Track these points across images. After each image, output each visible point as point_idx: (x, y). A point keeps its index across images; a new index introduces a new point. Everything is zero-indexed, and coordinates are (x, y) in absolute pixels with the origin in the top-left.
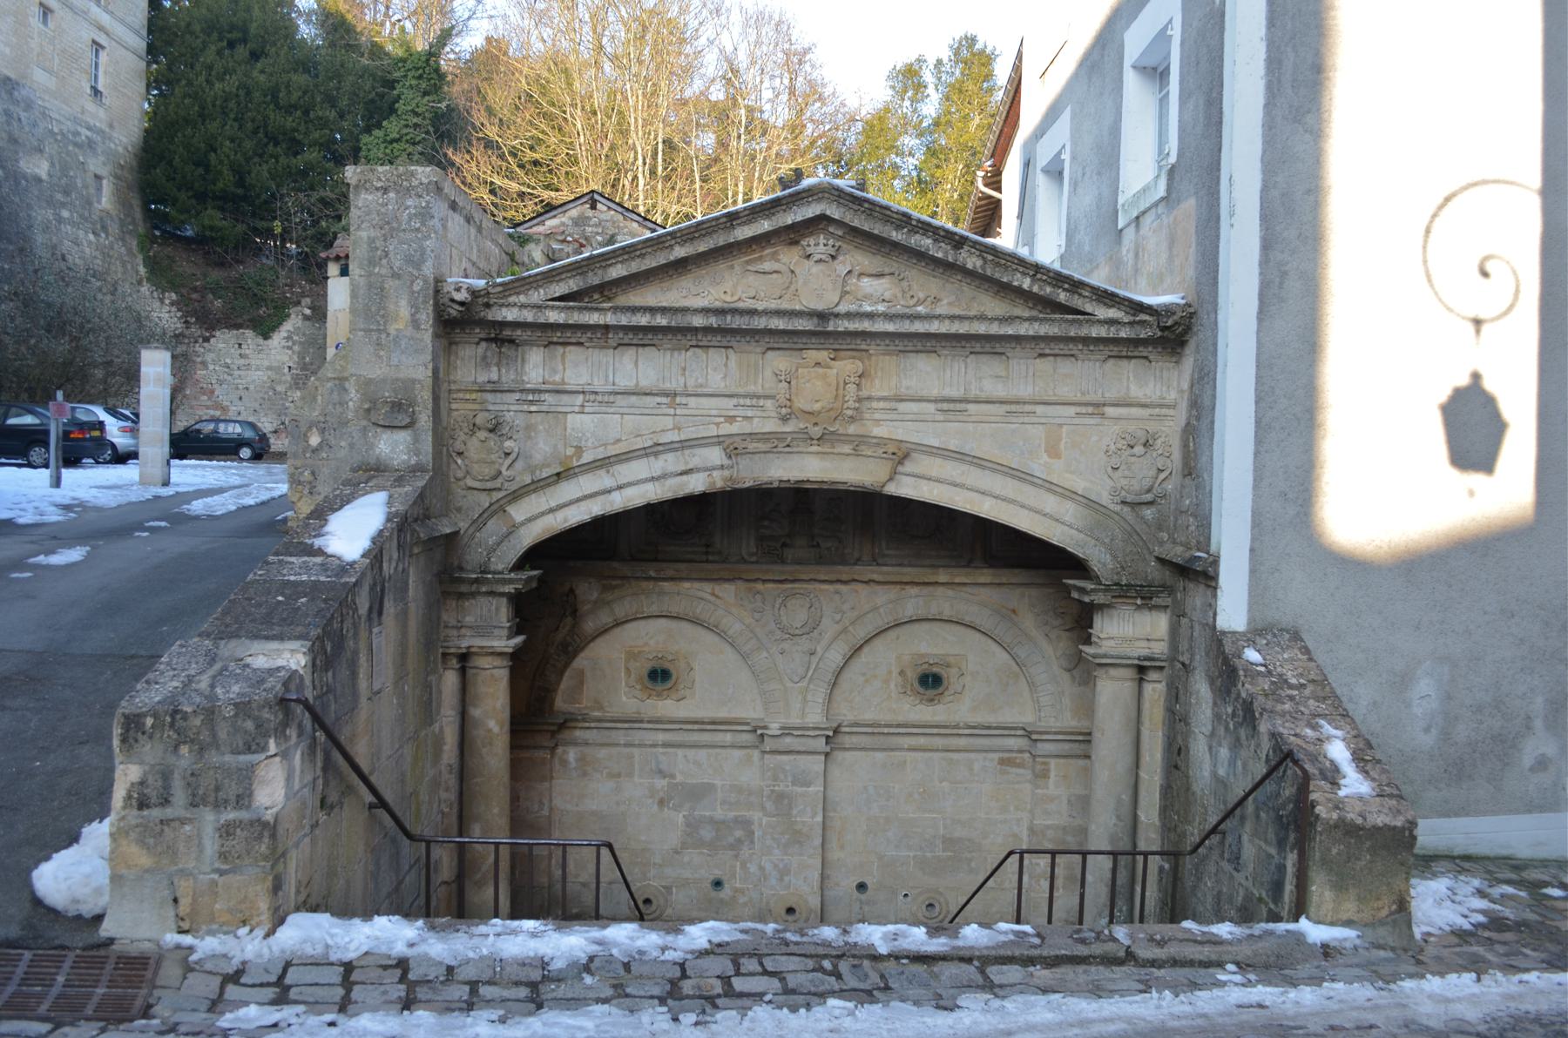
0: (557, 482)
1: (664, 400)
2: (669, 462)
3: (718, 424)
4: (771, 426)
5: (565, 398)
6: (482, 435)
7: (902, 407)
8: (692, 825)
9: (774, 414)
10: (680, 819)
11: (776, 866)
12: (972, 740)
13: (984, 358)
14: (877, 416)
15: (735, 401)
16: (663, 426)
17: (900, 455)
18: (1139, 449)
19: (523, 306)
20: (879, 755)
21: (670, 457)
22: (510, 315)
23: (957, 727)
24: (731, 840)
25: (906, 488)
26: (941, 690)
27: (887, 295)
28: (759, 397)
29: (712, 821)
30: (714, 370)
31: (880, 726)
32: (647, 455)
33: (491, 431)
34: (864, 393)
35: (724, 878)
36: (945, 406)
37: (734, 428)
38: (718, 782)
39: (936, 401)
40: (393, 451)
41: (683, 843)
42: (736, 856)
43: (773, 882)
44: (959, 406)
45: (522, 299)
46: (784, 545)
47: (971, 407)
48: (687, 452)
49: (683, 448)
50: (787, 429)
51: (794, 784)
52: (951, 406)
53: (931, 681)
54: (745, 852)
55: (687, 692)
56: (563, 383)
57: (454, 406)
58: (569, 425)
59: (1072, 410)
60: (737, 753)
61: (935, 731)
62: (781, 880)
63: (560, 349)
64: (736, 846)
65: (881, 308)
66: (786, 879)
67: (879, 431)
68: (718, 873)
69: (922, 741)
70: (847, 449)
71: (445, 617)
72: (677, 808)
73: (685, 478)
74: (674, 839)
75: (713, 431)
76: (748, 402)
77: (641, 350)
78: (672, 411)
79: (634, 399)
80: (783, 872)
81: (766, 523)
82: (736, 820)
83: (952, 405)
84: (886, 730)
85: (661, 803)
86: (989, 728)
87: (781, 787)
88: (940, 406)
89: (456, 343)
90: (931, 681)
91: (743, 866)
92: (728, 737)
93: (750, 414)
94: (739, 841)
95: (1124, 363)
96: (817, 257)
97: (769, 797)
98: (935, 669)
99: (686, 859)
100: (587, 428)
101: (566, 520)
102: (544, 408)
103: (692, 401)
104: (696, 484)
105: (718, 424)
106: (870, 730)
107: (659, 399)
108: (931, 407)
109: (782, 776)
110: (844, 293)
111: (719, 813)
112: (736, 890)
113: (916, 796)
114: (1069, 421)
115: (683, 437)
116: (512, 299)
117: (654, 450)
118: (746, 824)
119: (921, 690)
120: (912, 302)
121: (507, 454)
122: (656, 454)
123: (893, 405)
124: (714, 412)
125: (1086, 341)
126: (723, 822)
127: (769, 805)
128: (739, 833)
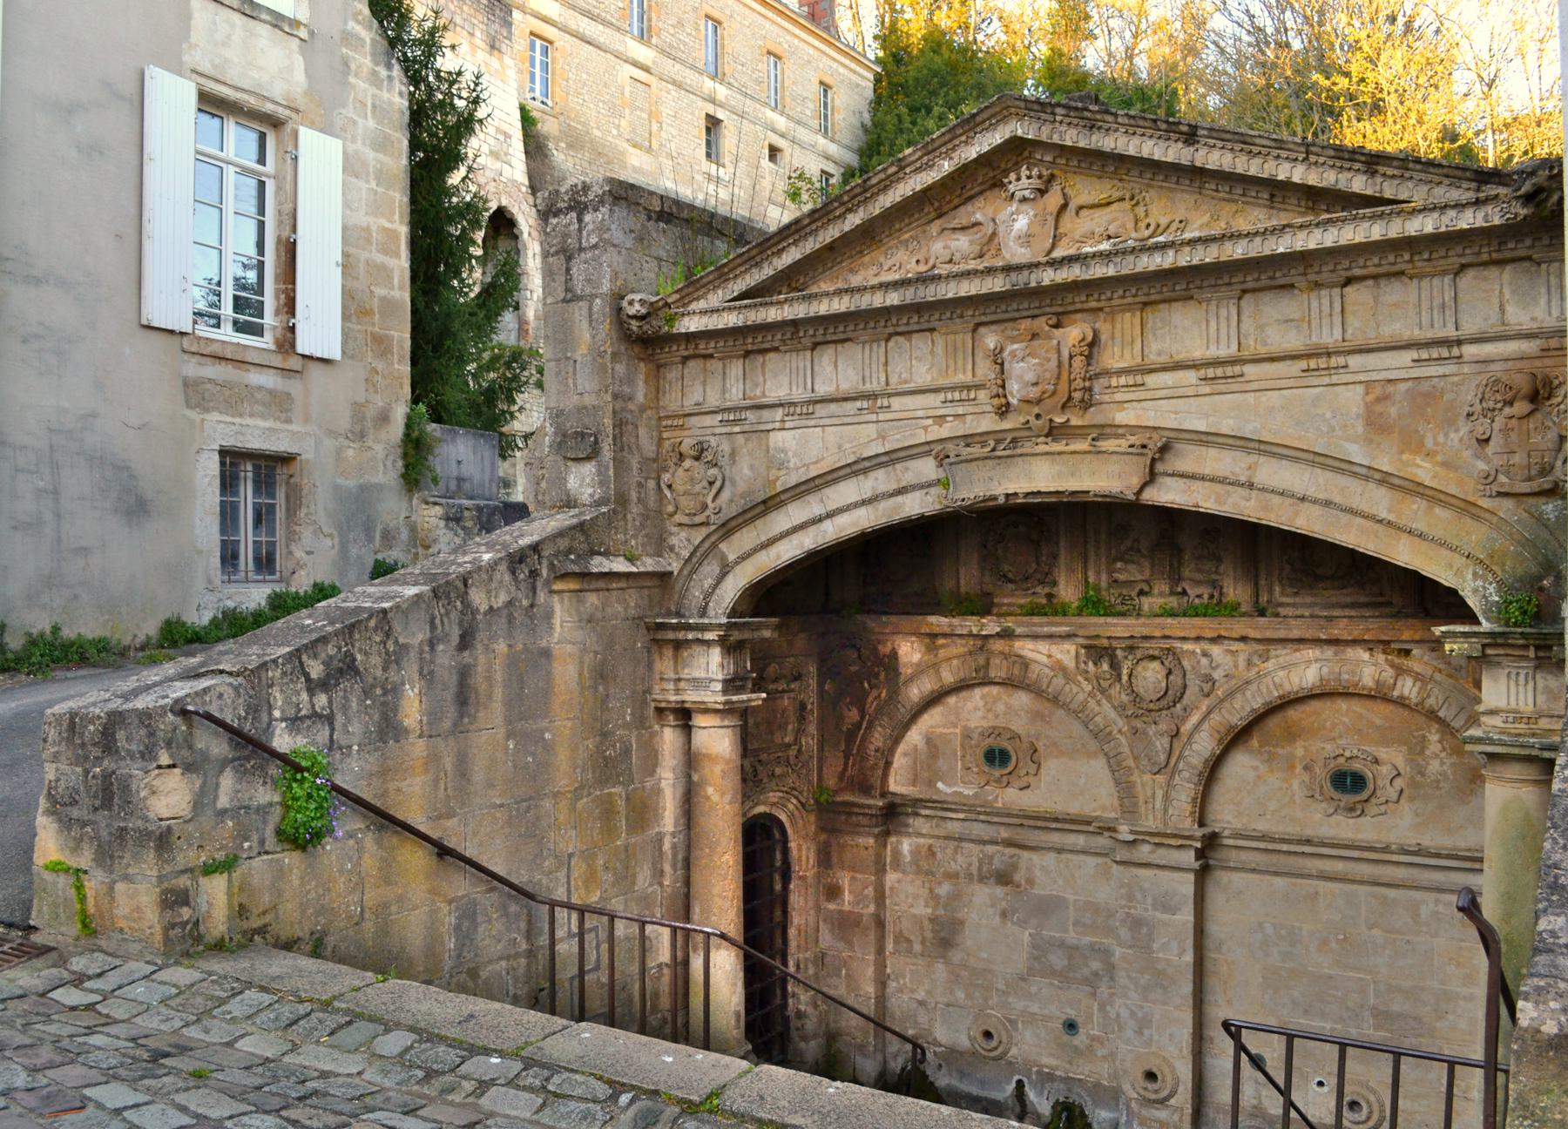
0: (763, 514)
1: (865, 404)
2: (879, 481)
3: (925, 428)
4: (988, 423)
5: (766, 414)
6: (687, 463)
7: (1152, 380)
8: (1040, 949)
9: (989, 408)
10: (1026, 938)
11: (1133, 1014)
12: (1415, 872)
13: (1266, 297)
14: (1118, 397)
15: (942, 396)
16: (865, 438)
17: (1158, 452)
18: (1521, 407)
19: (704, 312)
20: (1279, 882)
21: (880, 474)
22: (692, 324)
23: (1386, 849)
24: (1086, 972)
25: (1169, 494)
26: (1364, 795)
27: (1112, 230)
28: (969, 388)
29: (1062, 944)
30: (918, 361)
31: (1273, 840)
32: (855, 474)
33: (697, 458)
34: (1093, 369)
35: (1079, 1021)
36: (1210, 373)
37: (945, 431)
38: (1071, 898)
39: (1194, 366)
40: (581, 485)
41: (1030, 969)
42: (1094, 994)
43: (1129, 1033)
44: (1229, 371)
45: (702, 304)
46: (1141, 593)
47: (1250, 370)
48: (898, 466)
49: (893, 462)
50: (1006, 425)
51: (1155, 909)
52: (1219, 372)
53: (1348, 782)
54: (1104, 990)
55: (1031, 779)
56: (764, 396)
57: (665, 435)
58: (771, 445)
59: (1407, 357)
60: (1092, 861)
61: (1356, 854)
62: (1140, 1033)
63: (760, 359)
64: (1092, 981)
65: (1105, 246)
66: (1146, 1032)
67: (1123, 417)
68: (1072, 1013)
69: (1340, 866)
70: (1081, 445)
71: (658, 666)
72: (1022, 923)
73: (899, 499)
74: (1020, 961)
75: (921, 437)
76: (957, 396)
77: (839, 347)
78: (873, 417)
79: (833, 407)
80: (1144, 1024)
81: (1119, 565)
82: (1092, 946)
83: (1219, 371)
84: (1285, 847)
85: (1004, 914)
86: (1438, 856)
87: (1137, 911)
88: (1202, 373)
89: (665, 365)
90: (1348, 782)
91: (1102, 1007)
92: (1080, 841)
93: (960, 411)
94: (1096, 974)
95: (1493, 272)
96: (1018, 195)
97: (1123, 921)
98: (1357, 766)
99: (1034, 989)
100: (803, 447)
101: (778, 557)
102: (746, 428)
103: (896, 403)
104: (915, 506)
105: (925, 428)
106: (1262, 845)
107: (858, 404)
108: (1190, 377)
109: (1139, 896)
110: (1056, 239)
111: (1072, 936)
112: (1093, 1039)
113: (1334, 945)
114: (1403, 374)
115: (888, 448)
116: (694, 306)
117: (857, 468)
118: (1105, 954)
119: (1337, 795)
120: (1147, 233)
121: (711, 484)
122: (865, 471)
123: (1139, 379)
124: (920, 413)
125: (1411, 244)
126: (1077, 948)
127: (1124, 933)
128: (1095, 965)
